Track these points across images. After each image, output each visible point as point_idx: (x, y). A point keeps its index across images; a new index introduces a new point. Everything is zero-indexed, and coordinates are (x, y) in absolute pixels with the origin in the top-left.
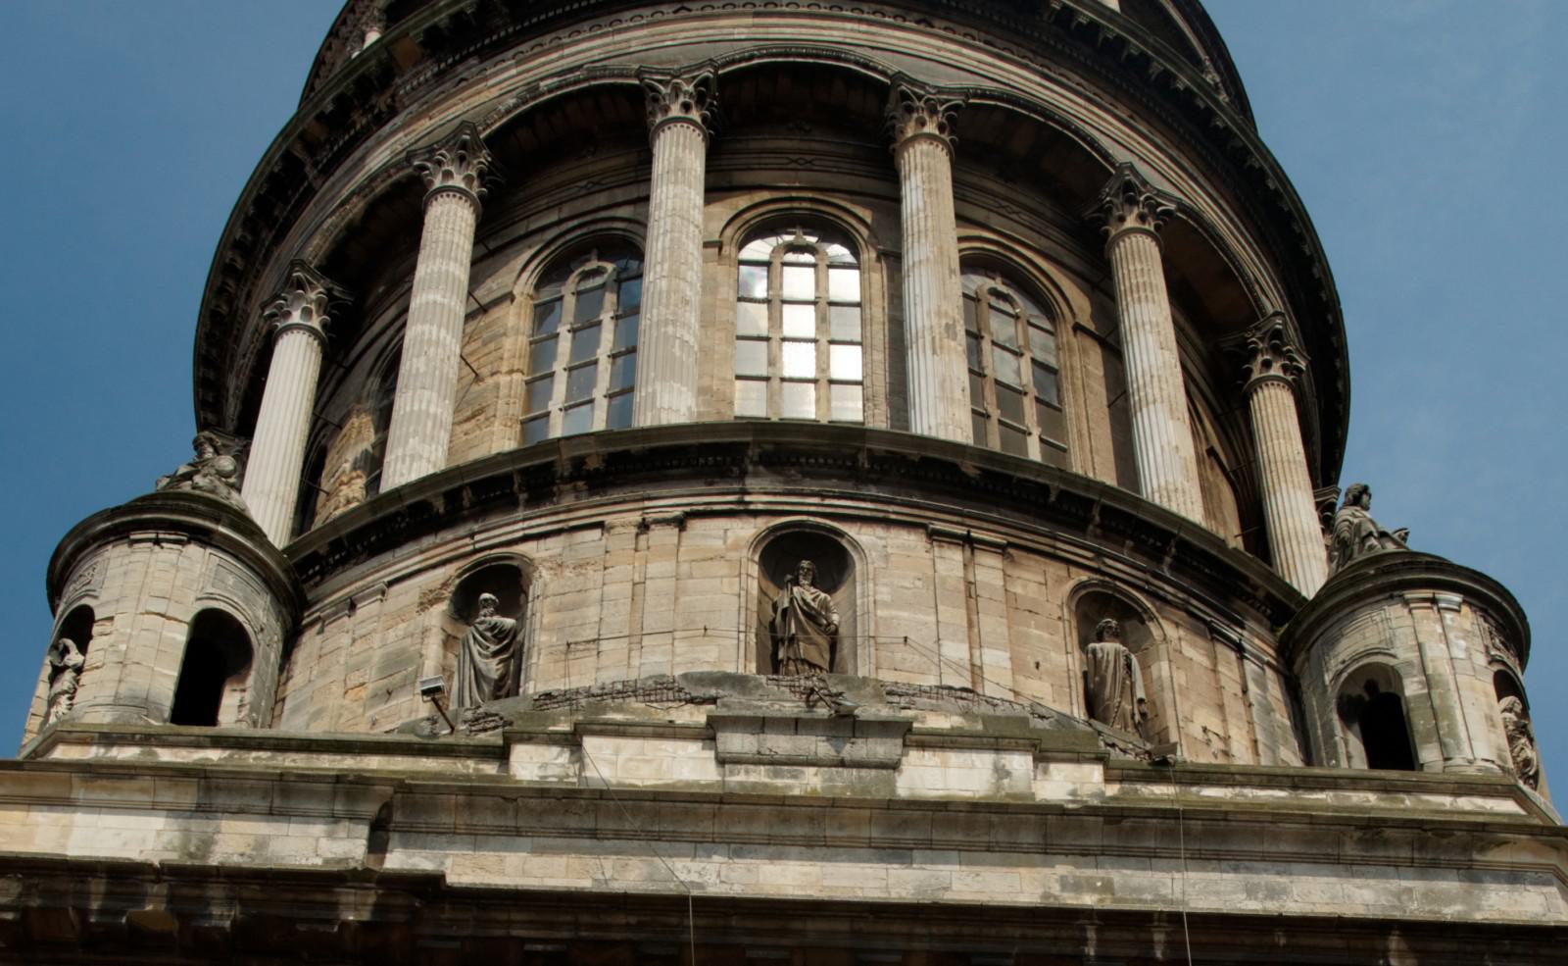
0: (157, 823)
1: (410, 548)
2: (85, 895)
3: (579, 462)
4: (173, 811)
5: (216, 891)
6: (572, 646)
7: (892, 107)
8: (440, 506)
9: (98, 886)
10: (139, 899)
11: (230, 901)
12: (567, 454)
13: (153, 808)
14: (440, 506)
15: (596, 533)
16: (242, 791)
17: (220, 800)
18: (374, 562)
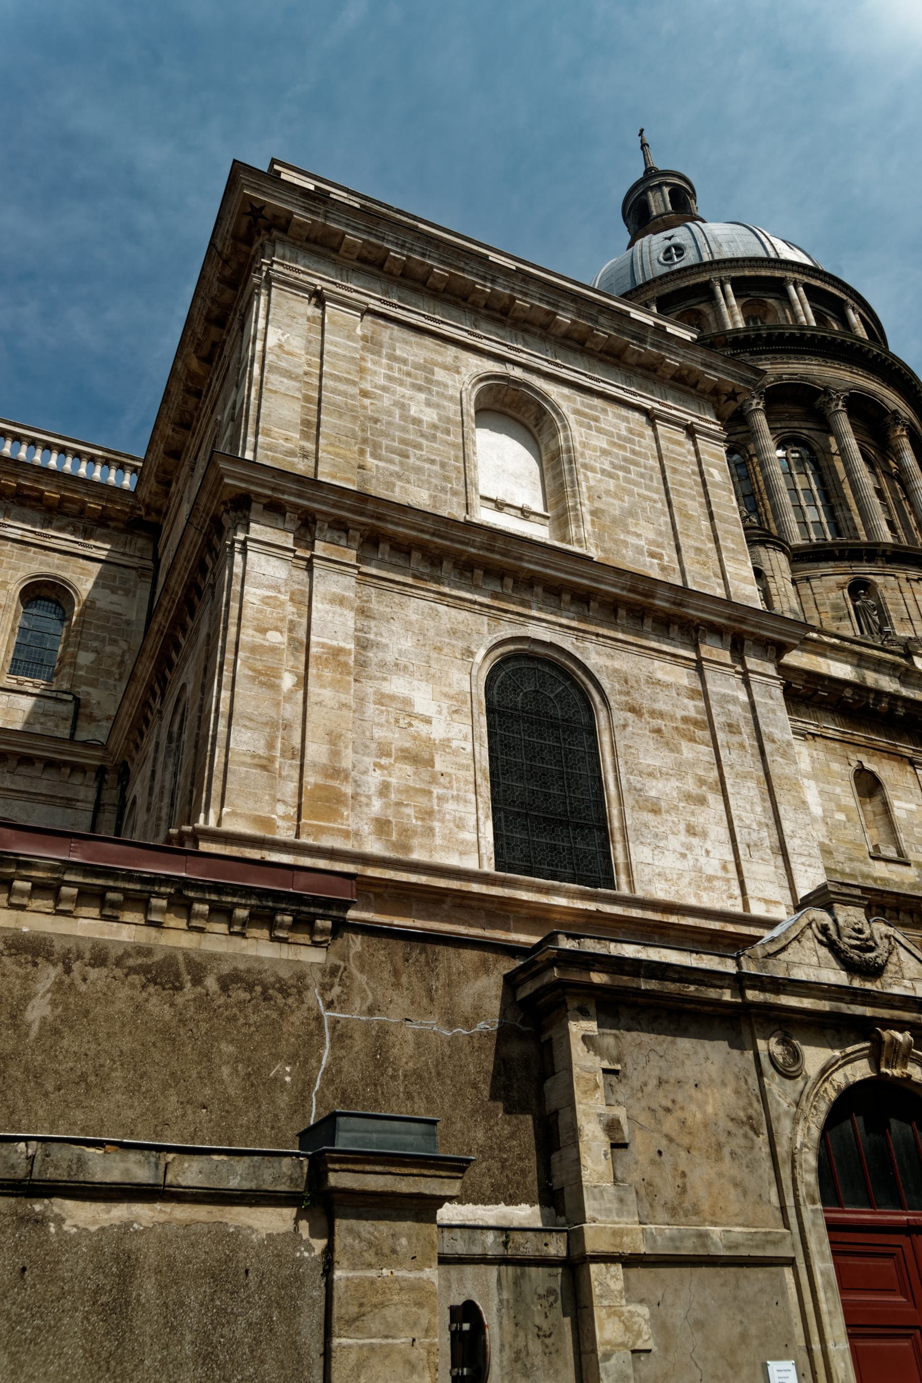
0: (848, 668)
1: (832, 564)
2: (868, 698)
3: (885, 551)
4: (851, 664)
5: (899, 703)
6: (195, 400)
7: (888, 419)
8: (837, 552)
9: (872, 696)
10: (881, 702)
11: (902, 707)
12: (882, 548)
13: (846, 662)
14: (837, 552)
15: (892, 578)
16: (868, 662)
17: (863, 664)
18: (815, 565)
